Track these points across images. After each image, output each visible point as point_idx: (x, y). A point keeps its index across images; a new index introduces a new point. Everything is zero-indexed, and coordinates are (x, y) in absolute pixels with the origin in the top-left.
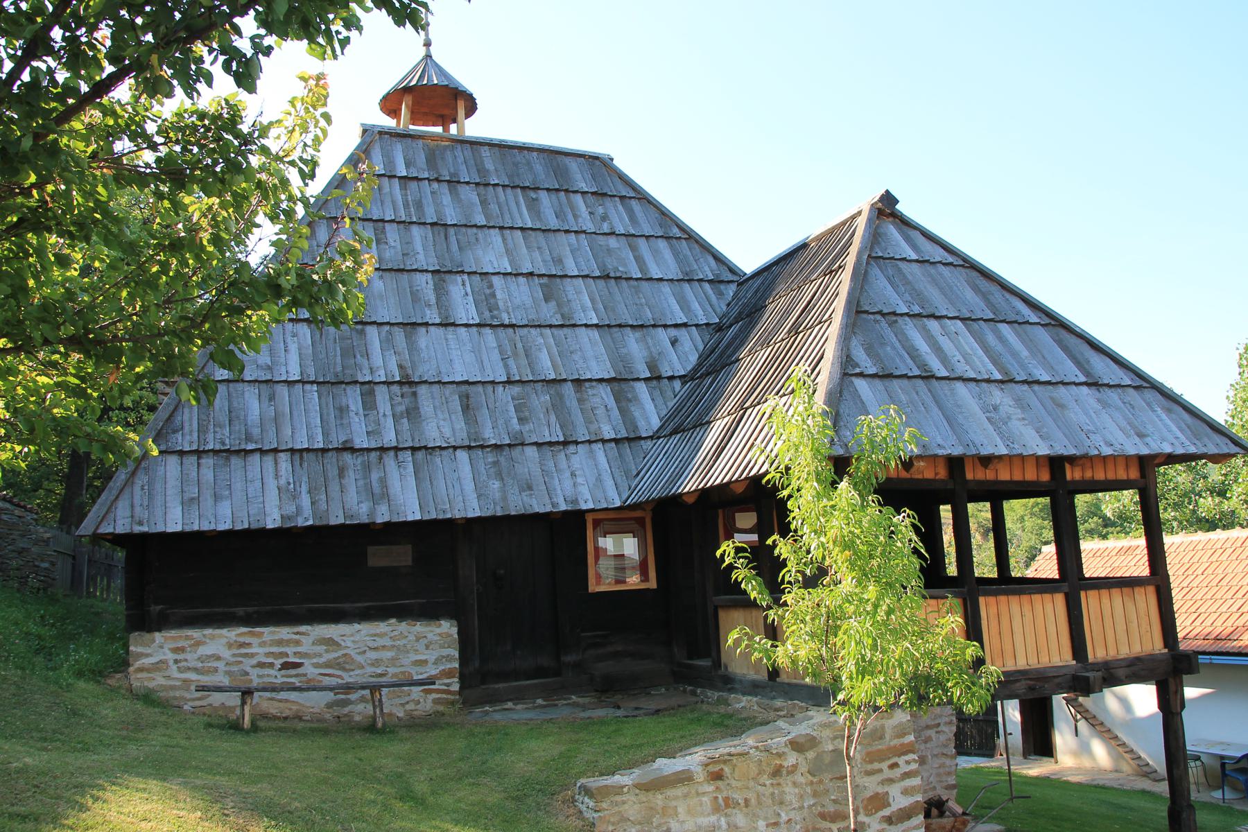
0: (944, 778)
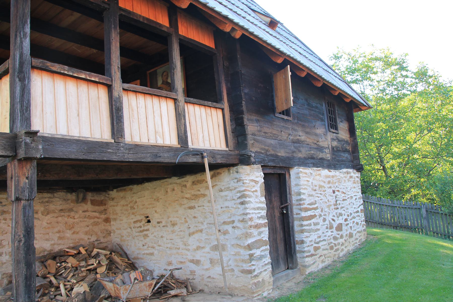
0: (240, 264)
